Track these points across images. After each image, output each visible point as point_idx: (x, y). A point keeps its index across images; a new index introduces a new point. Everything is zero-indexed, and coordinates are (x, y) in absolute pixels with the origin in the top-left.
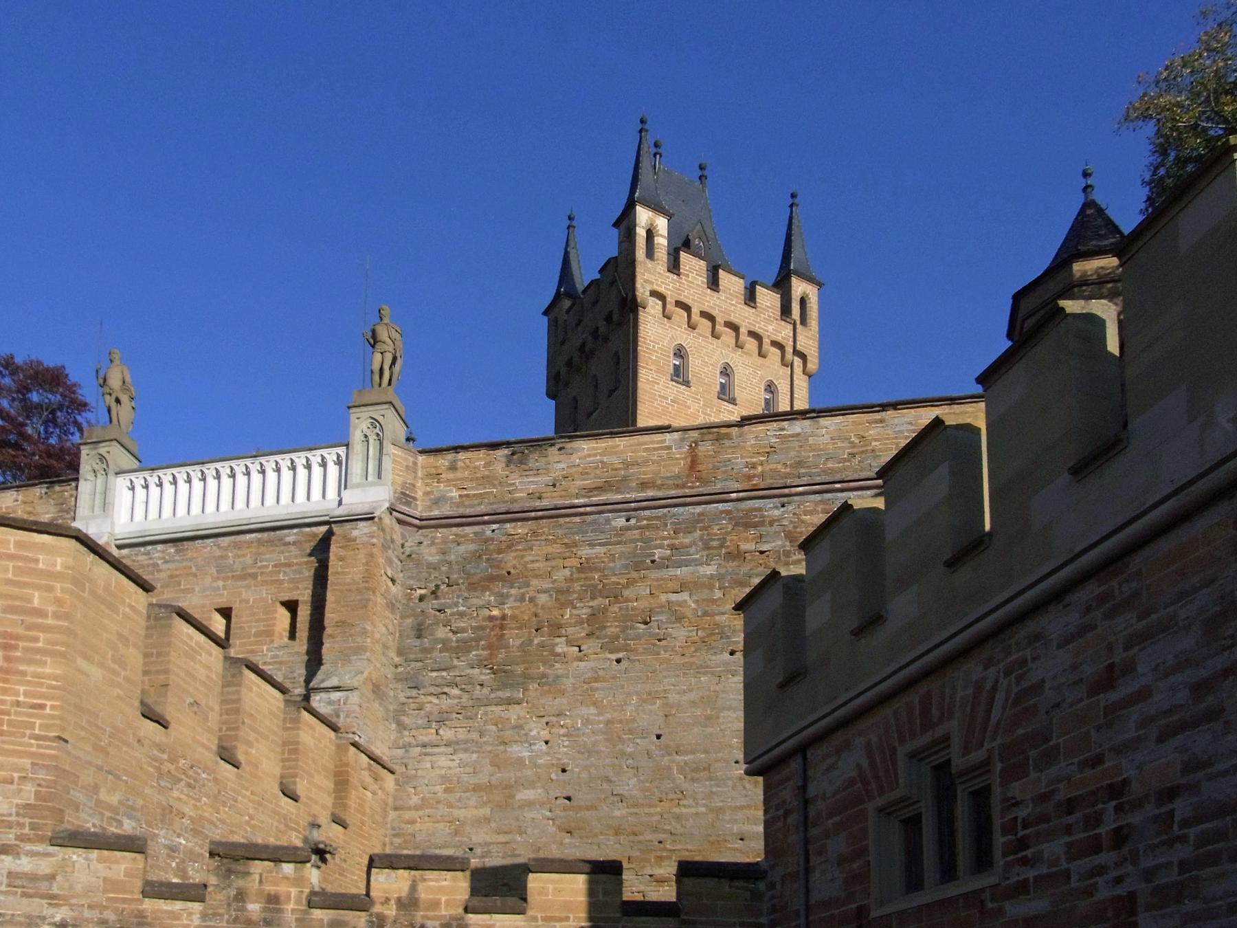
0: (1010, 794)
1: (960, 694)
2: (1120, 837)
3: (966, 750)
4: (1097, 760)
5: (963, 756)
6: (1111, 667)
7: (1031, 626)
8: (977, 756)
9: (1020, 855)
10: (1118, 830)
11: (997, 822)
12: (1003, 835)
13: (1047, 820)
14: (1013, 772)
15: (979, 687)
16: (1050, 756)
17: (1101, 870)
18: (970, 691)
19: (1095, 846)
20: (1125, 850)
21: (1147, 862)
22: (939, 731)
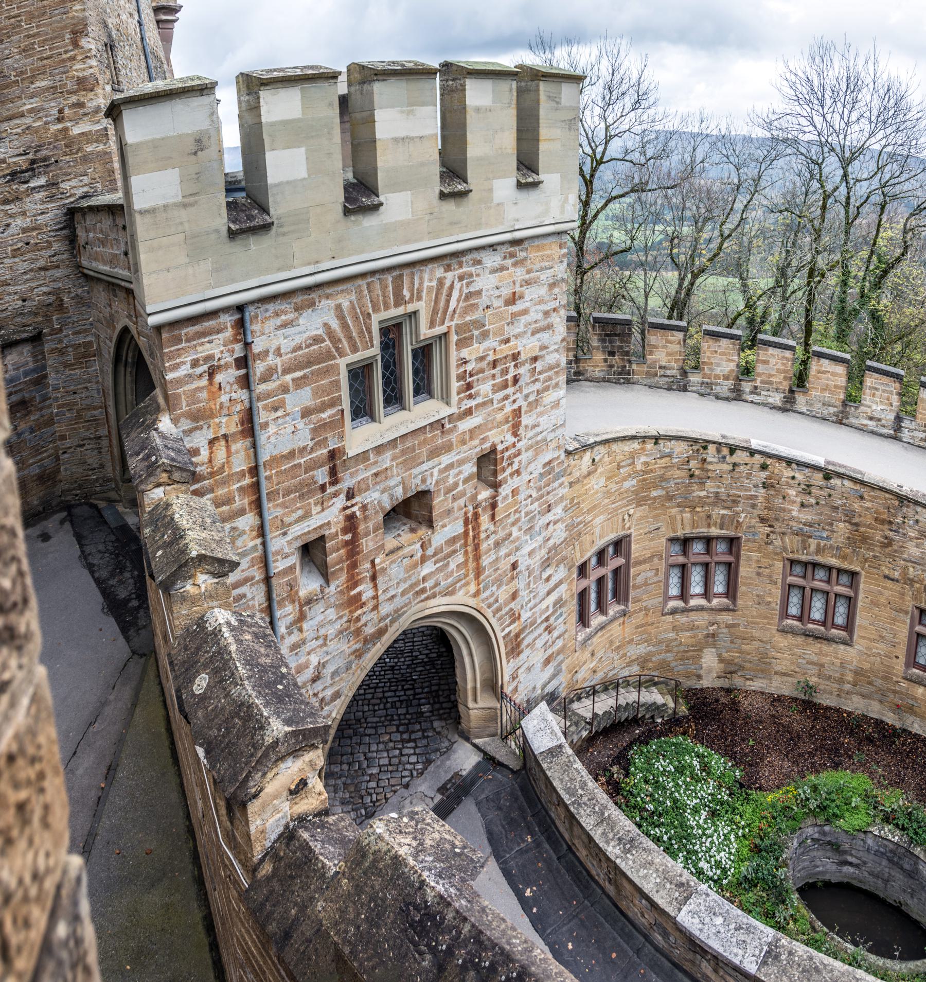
0: (462, 356)
1: (426, 284)
2: (516, 380)
3: (432, 324)
4: (507, 341)
5: (430, 328)
6: (514, 293)
7: (476, 255)
8: (439, 330)
9: (468, 393)
10: (515, 376)
11: (454, 373)
12: (458, 382)
13: (482, 371)
14: (461, 344)
15: (441, 282)
16: (485, 335)
17: (506, 398)
18: (434, 283)
19: (505, 386)
20: (517, 386)
21: (525, 392)
22: (410, 308)
